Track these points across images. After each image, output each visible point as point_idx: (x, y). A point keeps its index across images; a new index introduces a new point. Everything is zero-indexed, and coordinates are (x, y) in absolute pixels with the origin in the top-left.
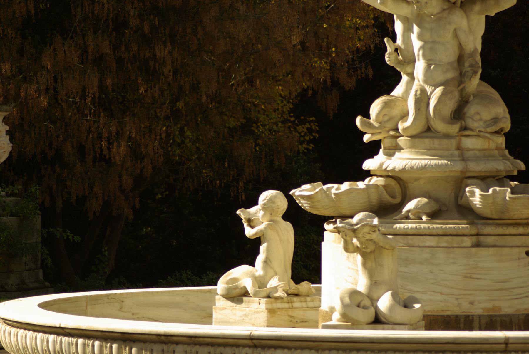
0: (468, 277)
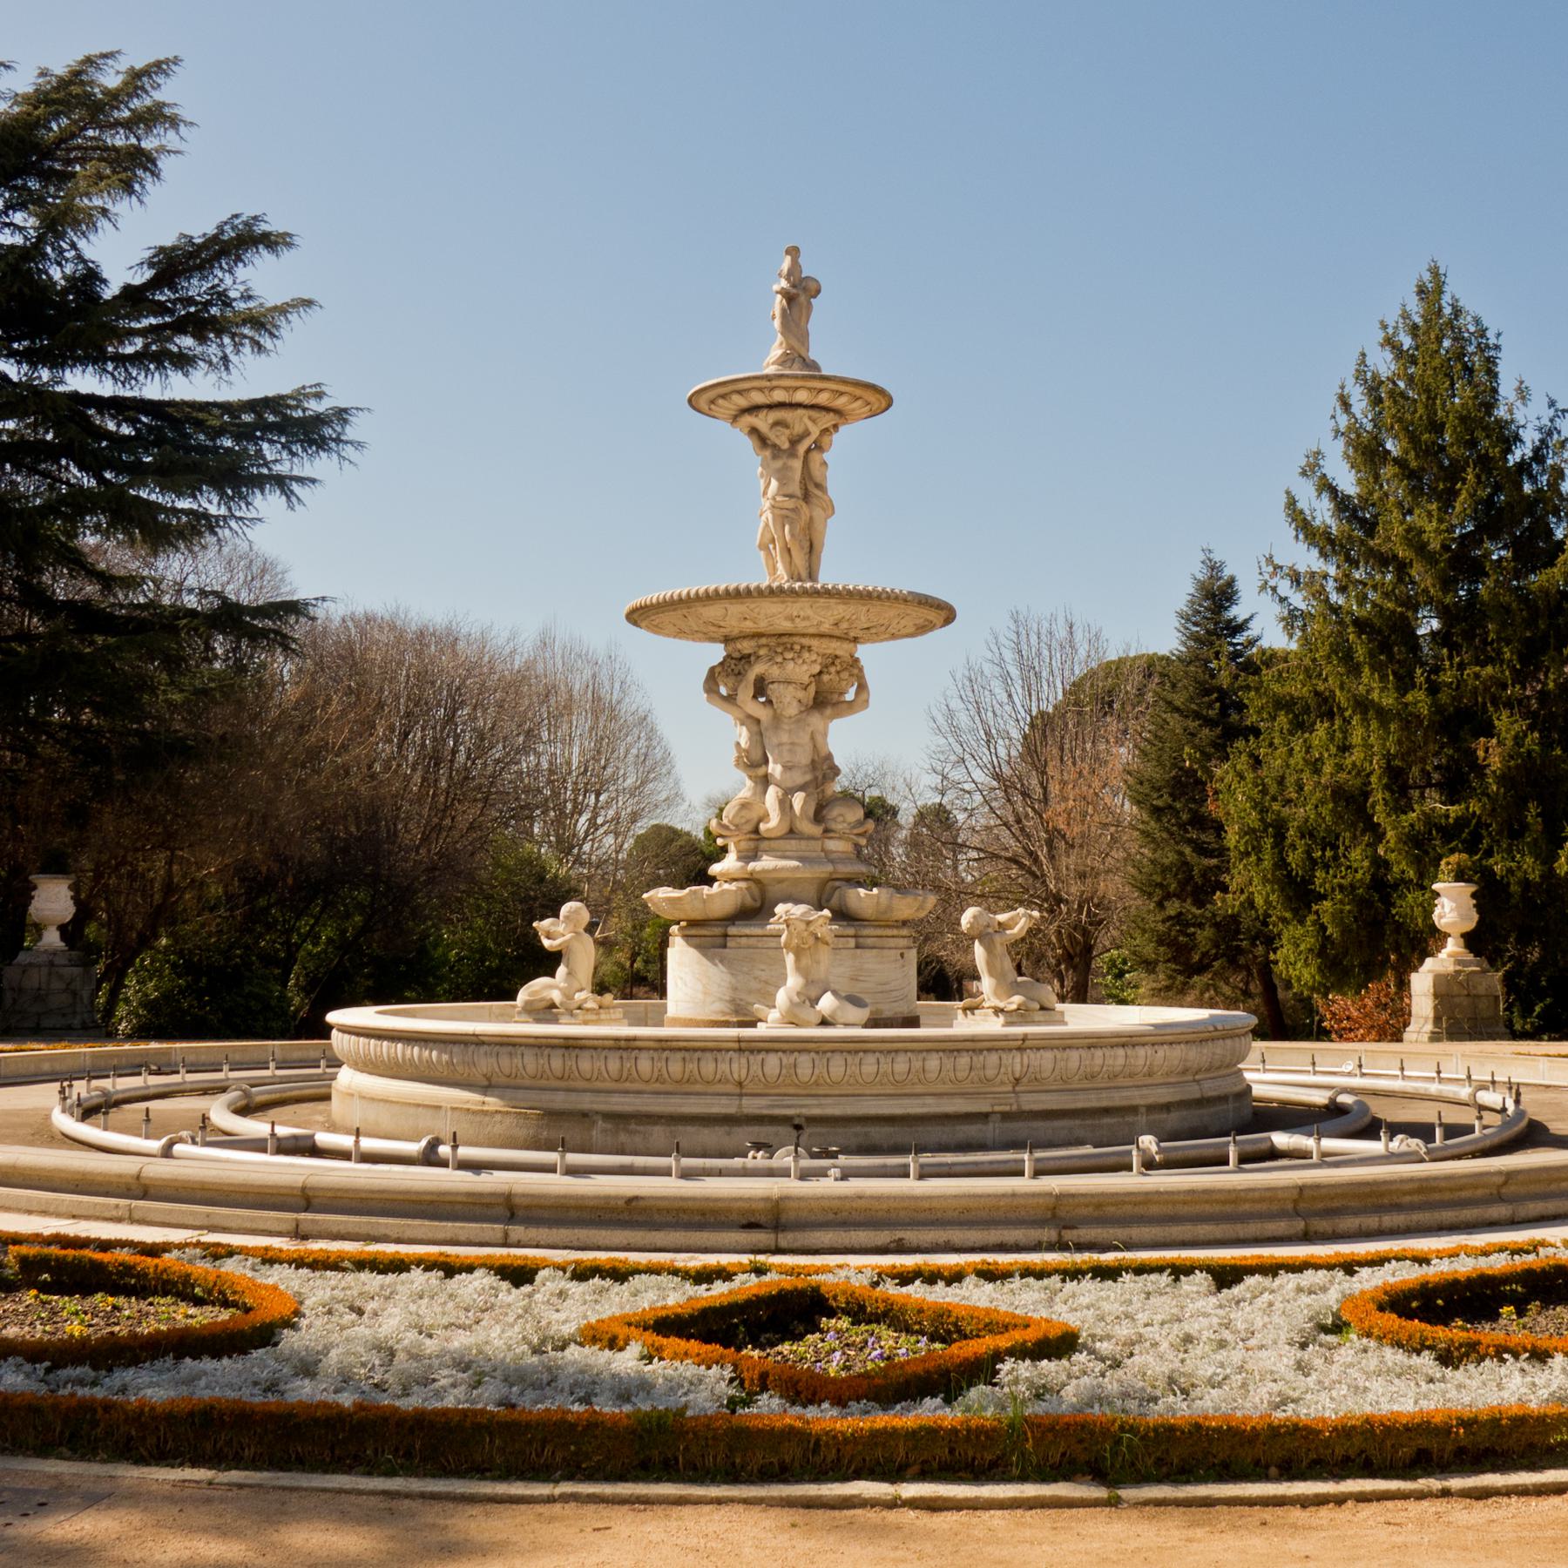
0: (854, 979)
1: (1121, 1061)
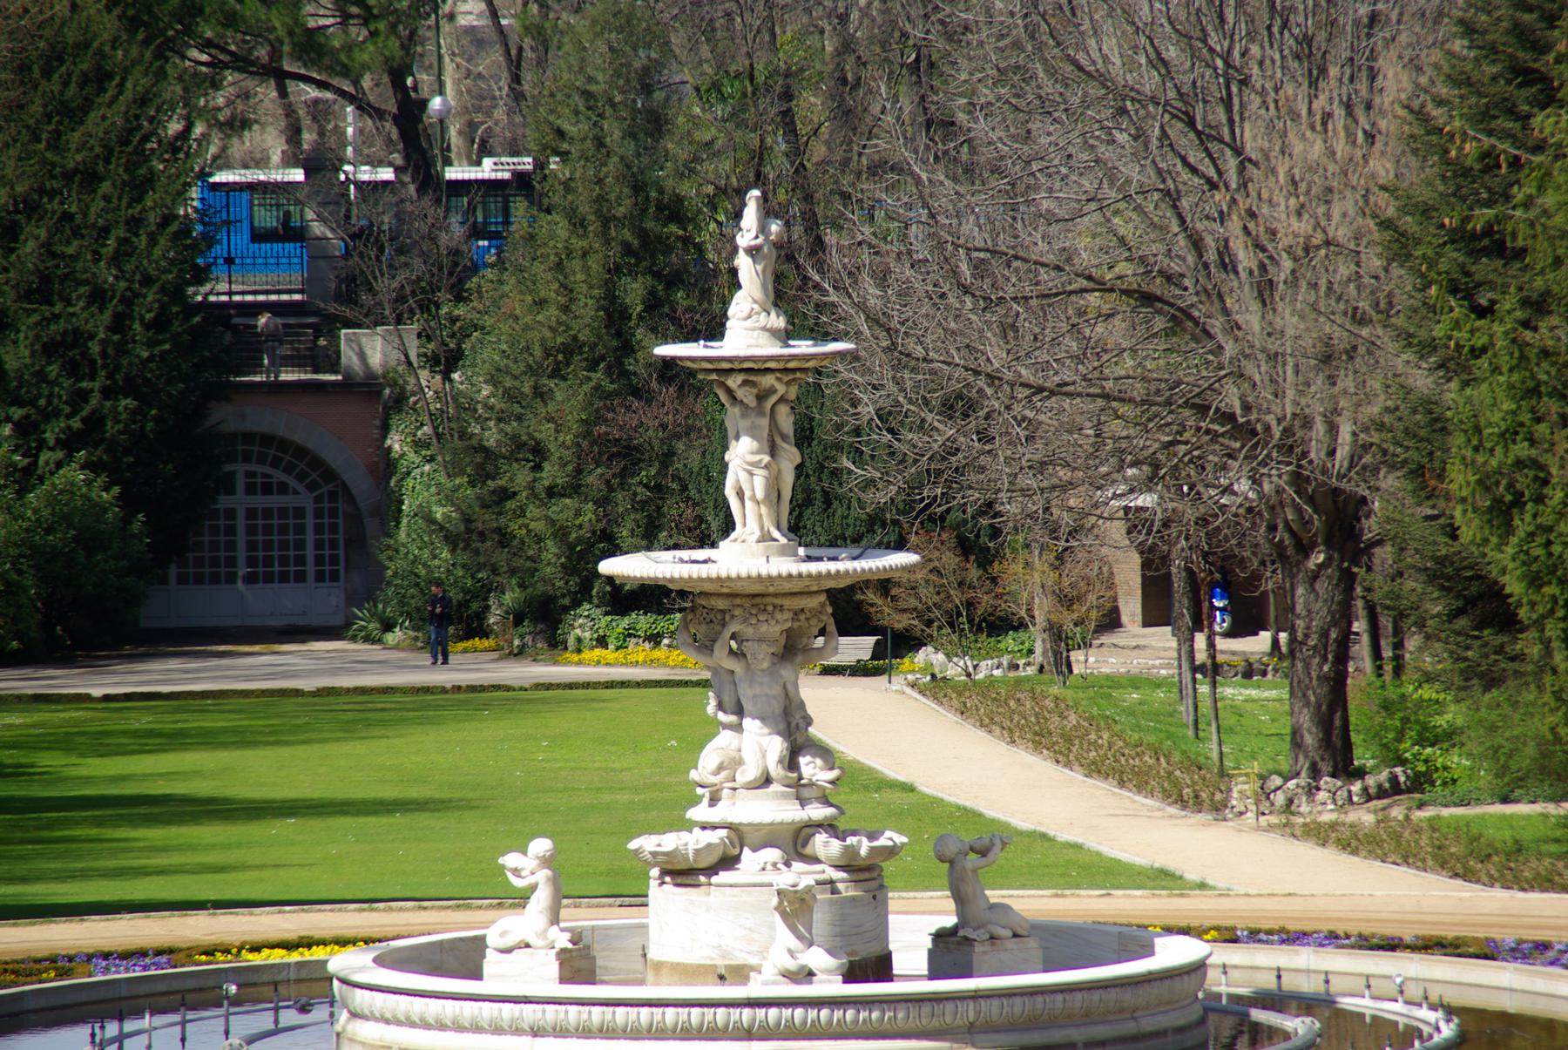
1: (1060, 1005)
